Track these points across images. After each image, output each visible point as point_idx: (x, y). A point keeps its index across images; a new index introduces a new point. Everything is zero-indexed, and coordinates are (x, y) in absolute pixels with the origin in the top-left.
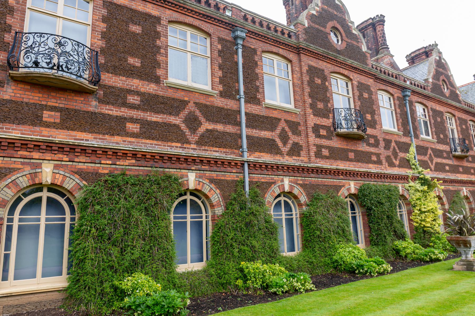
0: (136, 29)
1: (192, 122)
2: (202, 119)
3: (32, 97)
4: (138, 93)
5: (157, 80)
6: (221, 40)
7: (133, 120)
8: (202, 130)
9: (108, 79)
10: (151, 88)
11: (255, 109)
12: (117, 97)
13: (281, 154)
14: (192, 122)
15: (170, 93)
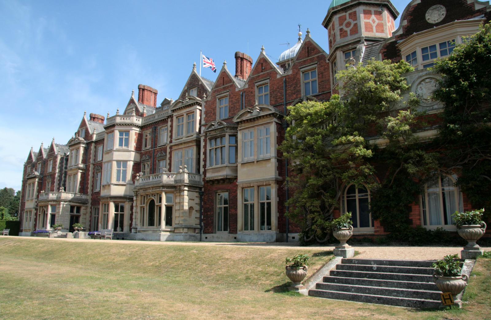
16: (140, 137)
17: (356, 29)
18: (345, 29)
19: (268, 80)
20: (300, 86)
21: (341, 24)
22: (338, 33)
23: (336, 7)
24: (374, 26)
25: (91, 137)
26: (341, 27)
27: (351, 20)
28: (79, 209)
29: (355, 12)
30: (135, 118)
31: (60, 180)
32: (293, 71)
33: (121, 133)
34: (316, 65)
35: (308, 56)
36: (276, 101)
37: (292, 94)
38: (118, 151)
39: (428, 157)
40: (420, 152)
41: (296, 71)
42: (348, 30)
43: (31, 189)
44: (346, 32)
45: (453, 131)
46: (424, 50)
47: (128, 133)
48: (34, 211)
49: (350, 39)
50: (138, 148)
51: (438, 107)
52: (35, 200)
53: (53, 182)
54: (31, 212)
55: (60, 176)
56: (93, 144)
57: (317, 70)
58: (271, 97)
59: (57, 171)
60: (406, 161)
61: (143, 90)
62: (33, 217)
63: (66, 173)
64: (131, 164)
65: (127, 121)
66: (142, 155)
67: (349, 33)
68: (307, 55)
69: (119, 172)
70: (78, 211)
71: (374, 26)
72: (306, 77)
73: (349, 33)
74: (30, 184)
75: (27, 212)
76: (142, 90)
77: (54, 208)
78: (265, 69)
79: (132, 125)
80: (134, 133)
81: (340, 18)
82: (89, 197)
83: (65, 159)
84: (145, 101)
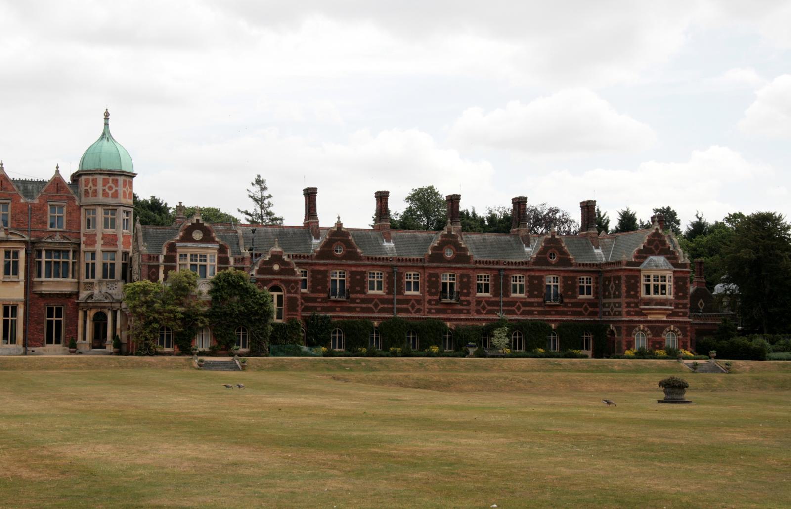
0: (358, 277)
1: (376, 305)
2: (379, 304)
3: (334, 305)
4: (360, 299)
5: (365, 293)
6: (387, 272)
7: (358, 307)
8: (379, 308)
9: (352, 296)
10: (363, 296)
11: (400, 297)
12: (353, 301)
13: (411, 313)
14: (376, 305)
15: (369, 297)
17: (115, 195)
18: (107, 190)
19: (10, 201)
20: (47, 218)
21: (104, 185)
22: (100, 192)
23: (104, 171)
26: (104, 188)
27: (113, 185)
29: (117, 180)
32: (40, 201)
34: (65, 204)
35: (57, 193)
36: (18, 225)
37: (37, 223)
39: (206, 320)
40: (202, 318)
41: (43, 202)
42: (110, 192)
44: (108, 193)
45: (217, 312)
46: (192, 255)
49: (110, 201)
51: (209, 298)
57: (65, 208)
58: (12, 219)
60: (196, 320)
67: (110, 195)
68: (56, 191)
72: (53, 211)
73: (110, 195)
78: (6, 189)
81: (104, 179)
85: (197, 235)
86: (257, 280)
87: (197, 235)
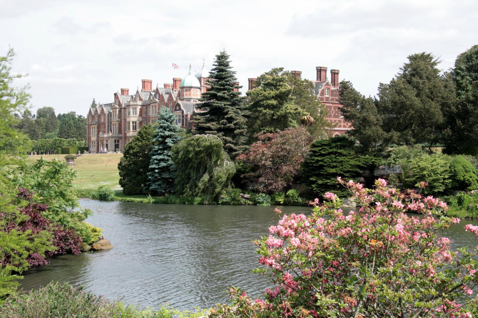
16: (141, 110)
24: (188, 94)
25: (122, 105)
28: (118, 141)
30: (138, 102)
31: (108, 126)
33: (133, 109)
38: (132, 117)
43: (94, 130)
47: (136, 109)
48: (96, 142)
50: (141, 115)
52: (96, 136)
53: (105, 127)
54: (95, 142)
55: (108, 124)
56: (123, 109)
59: (106, 121)
61: (144, 82)
62: (96, 145)
63: (111, 123)
64: (138, 122)
65: (135, 103)
66: (143, 118)
69: (133, 126)
70: (118, 142)
71: (188, 94)
74: (92, 128)
75: (92, 142)
76: (144, 82)
77: (107, 141)
79: (137, 105)
80: (139, 108)
82: (123, 135)
83: (110, 114)
84: (146, 88)
85: (178, 108)
86: (190, 123)
87: (178, 108)
